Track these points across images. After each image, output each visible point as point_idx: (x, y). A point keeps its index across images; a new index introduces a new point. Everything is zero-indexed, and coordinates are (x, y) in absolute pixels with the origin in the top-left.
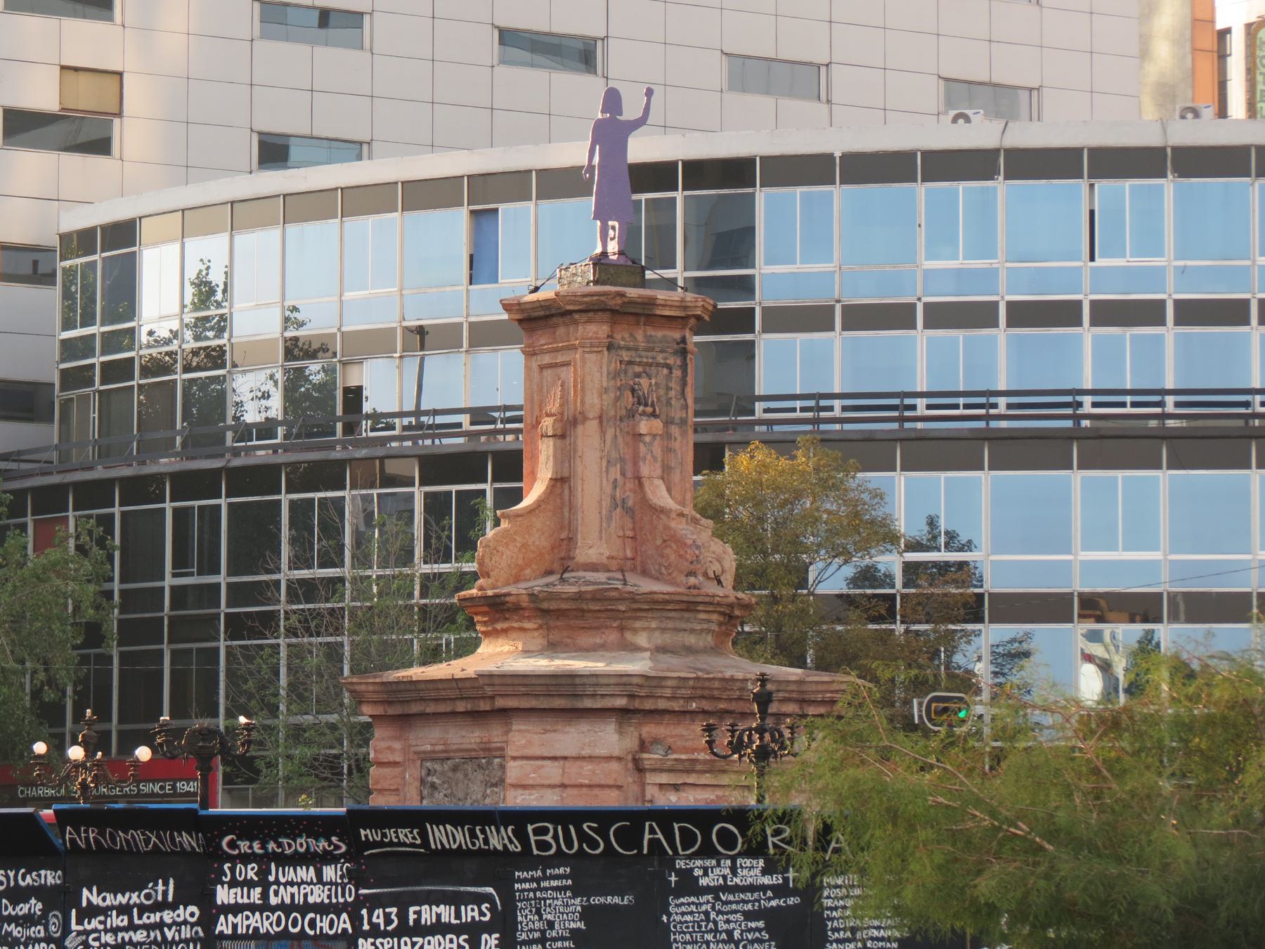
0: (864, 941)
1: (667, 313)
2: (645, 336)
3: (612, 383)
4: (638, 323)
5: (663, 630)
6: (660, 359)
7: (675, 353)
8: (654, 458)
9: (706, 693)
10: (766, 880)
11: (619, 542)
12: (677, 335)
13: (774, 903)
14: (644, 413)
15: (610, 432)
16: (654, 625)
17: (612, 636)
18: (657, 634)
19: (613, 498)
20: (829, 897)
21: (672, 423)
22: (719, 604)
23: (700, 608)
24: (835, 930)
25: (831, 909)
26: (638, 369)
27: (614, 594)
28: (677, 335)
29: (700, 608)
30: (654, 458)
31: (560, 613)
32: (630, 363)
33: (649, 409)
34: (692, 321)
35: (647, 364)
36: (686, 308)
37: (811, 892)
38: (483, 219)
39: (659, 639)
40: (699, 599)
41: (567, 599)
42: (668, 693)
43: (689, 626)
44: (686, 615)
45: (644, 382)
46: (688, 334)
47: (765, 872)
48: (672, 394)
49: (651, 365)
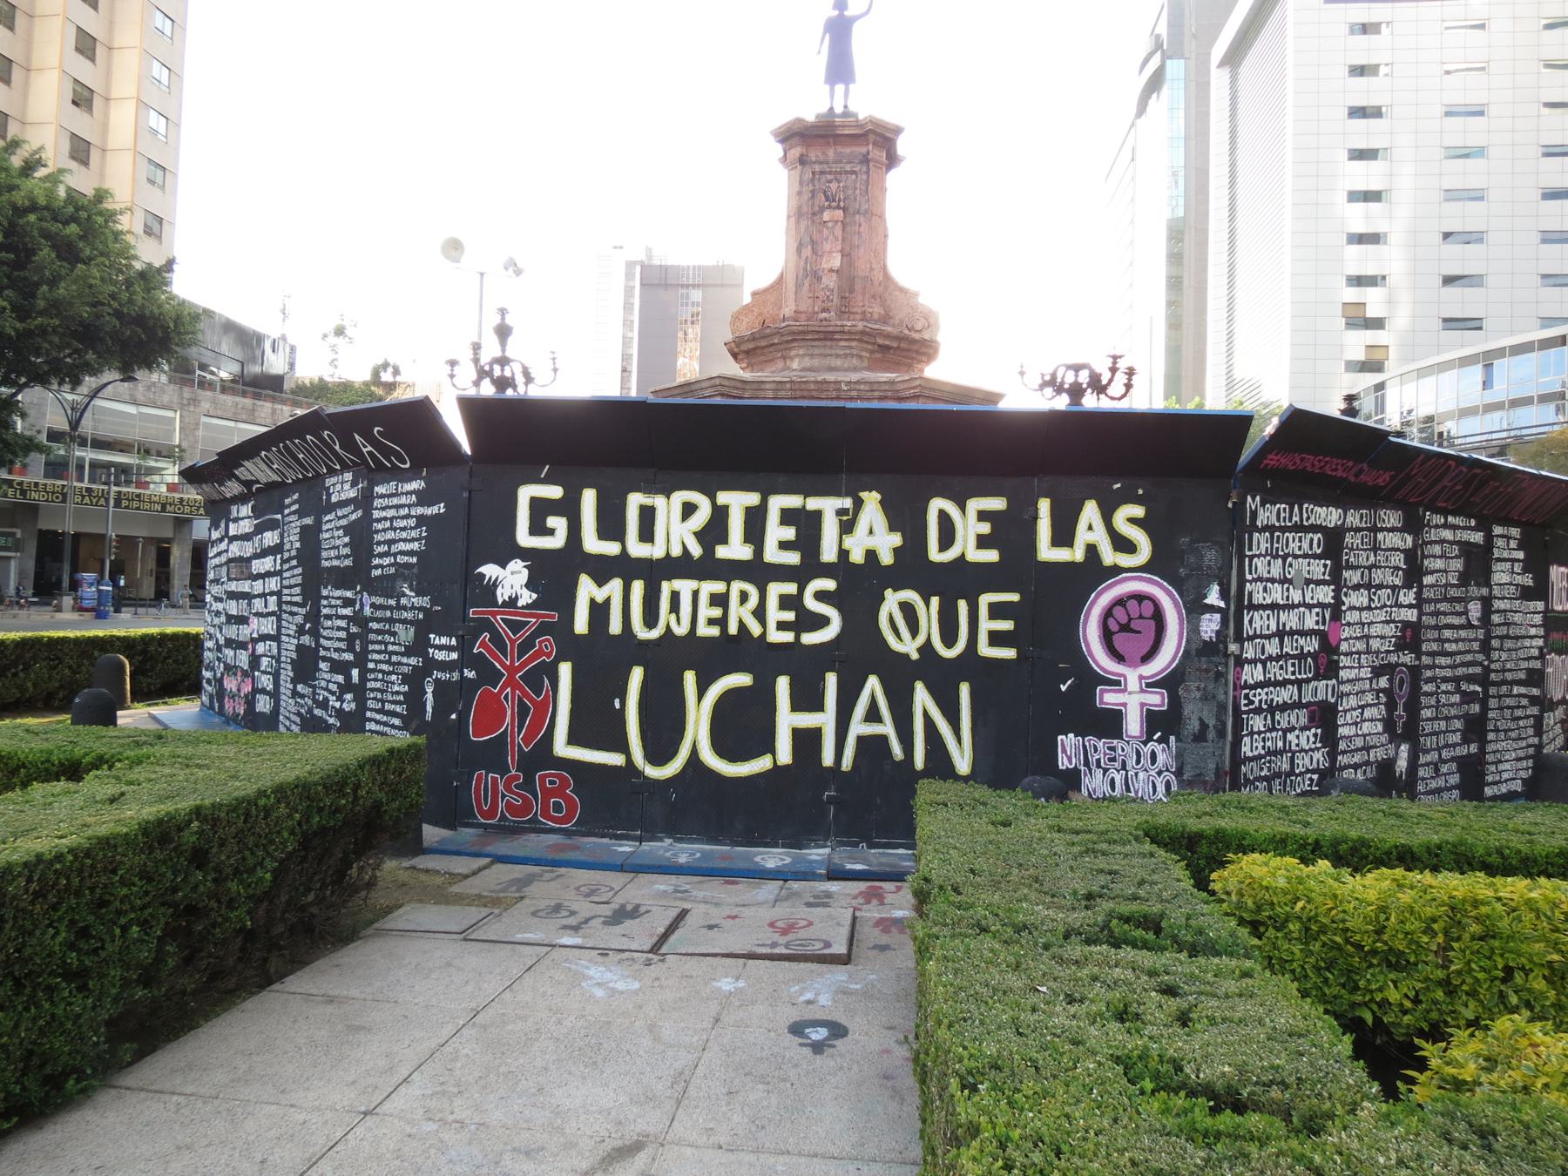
0: (395, 555)
1: (847, 132)
2: (835, 153)
3: (805, 189)
4: (828, 144)
5: (812, 356)
6: (848, 168)
7: (861, 162)
8: (837, 239)
9: (805, 394)
10: (352, 494)
11: (810, 301)
12: (863, 150)
13: (353, 517)
14: (830, 207)
15: (804, 223)
16: (801, 352)
17: (780, 364)
18: (807, 359)
19: (805, 270)
20: (376, 509)
21: (858, 213)
22: (850, 332)
23: (837, 336)
24: (379, 543)
25: (379, 520)
26: (829, 177)
27: (768, 331)
28: (863, 150)
29: (837, 336)
30: (837, 239)
31: (747, 352)
32: (822, 173)
33: (834, 204)
34: (872, 137)
35: (836, 172)
36: (862, 126)
37: (365, 501)
38: (1488, 367)
39: (807, 362)
40: (830, 329)
41: (748, 340)
42: (770, 394)
43: (833, 352)
44: (829, 343)
45: (834, 186)
46: (871, 147)
47: (352, 486)
48: (858, 192)
49: (840, 173)
